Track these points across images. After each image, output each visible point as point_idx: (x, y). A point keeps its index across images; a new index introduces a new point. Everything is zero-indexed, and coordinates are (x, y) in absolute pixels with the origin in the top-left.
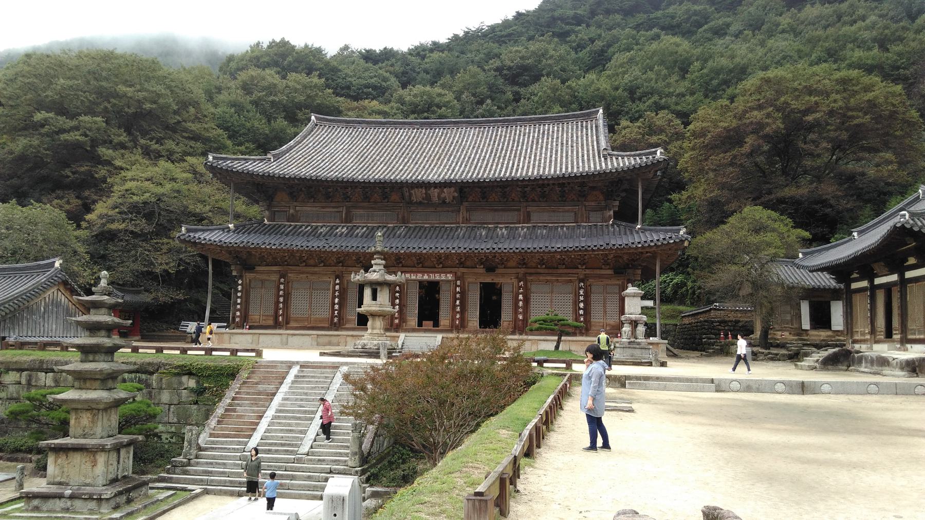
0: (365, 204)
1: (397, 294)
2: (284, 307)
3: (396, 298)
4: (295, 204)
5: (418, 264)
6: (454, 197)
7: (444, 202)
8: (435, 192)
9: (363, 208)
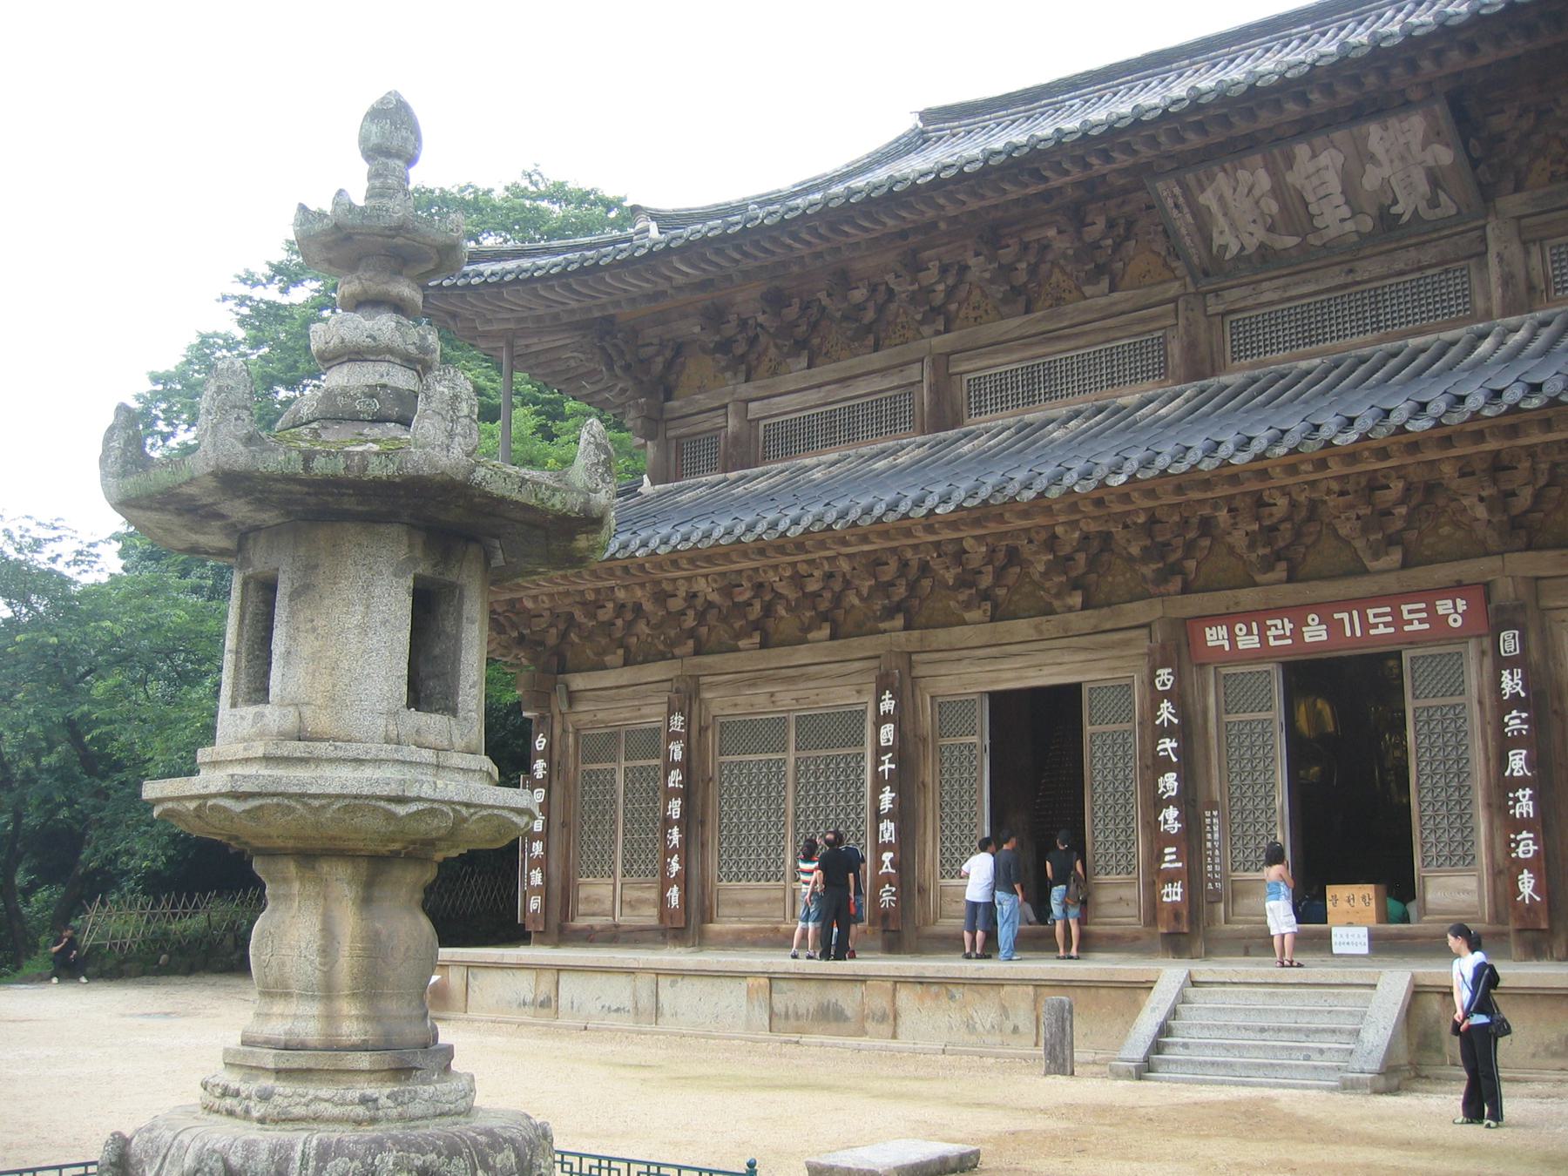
0: (1014, 325)
1: (1168, 744)
2: (685, 841)
3: (1162, 766)
4: (745, 390)
5: (1268, 566)
6: (1435, 179)
7: (1387, 221)
8: (1318, 169)
9: (996, 345)
